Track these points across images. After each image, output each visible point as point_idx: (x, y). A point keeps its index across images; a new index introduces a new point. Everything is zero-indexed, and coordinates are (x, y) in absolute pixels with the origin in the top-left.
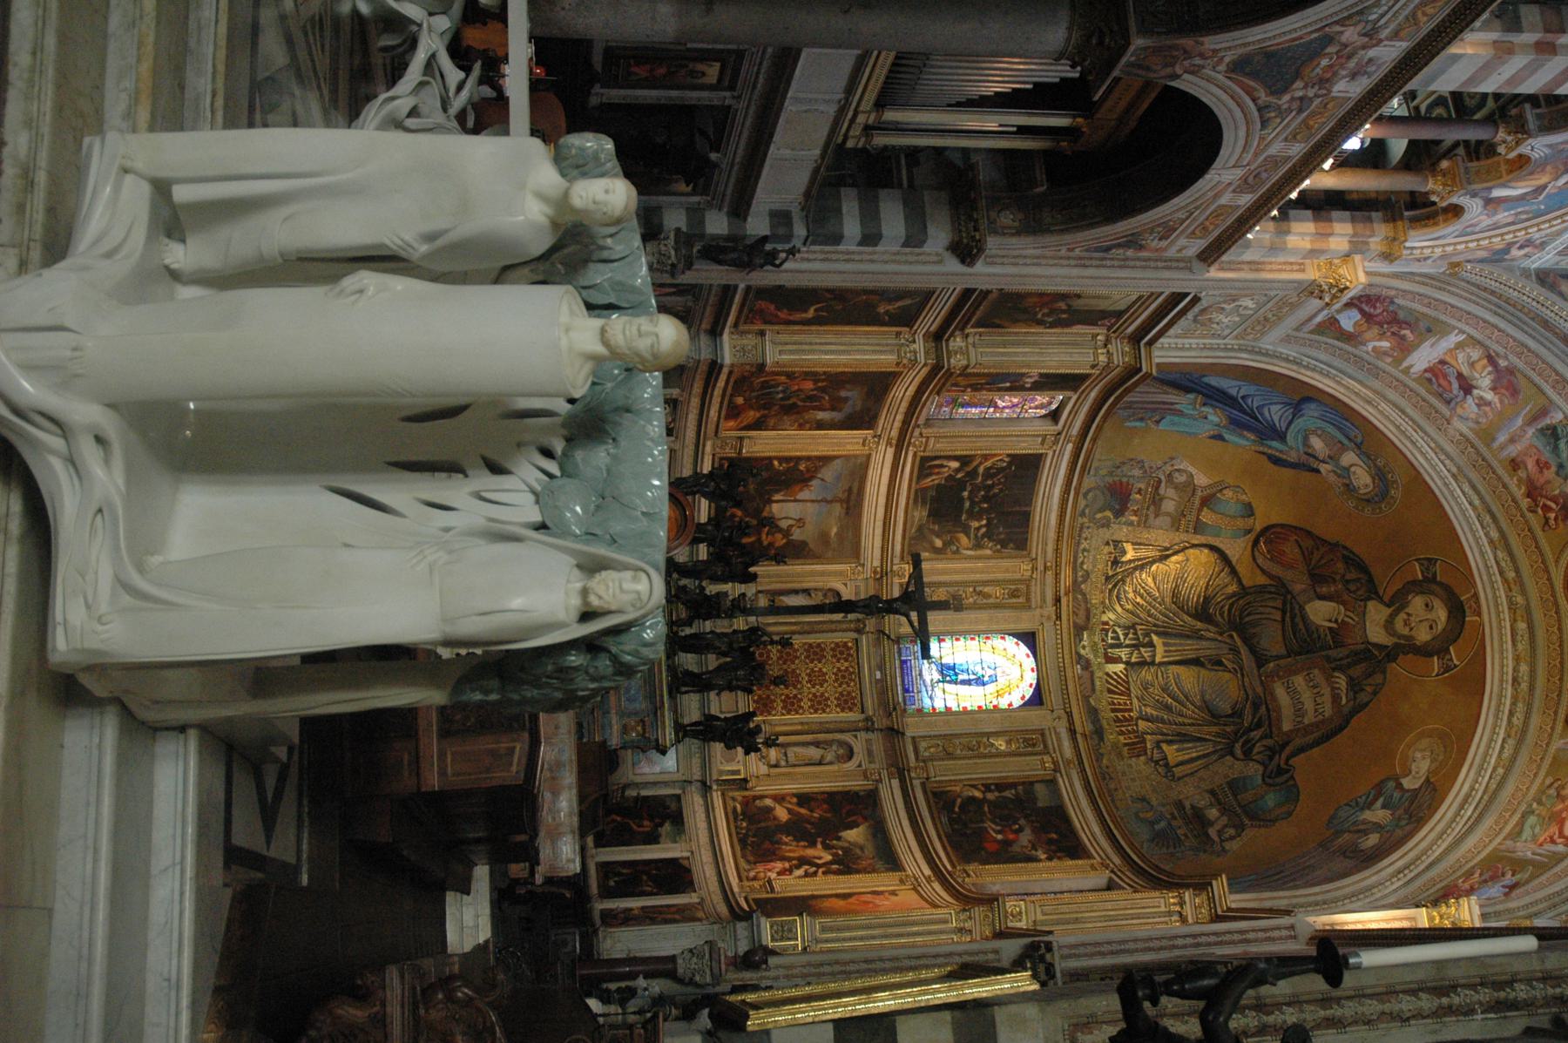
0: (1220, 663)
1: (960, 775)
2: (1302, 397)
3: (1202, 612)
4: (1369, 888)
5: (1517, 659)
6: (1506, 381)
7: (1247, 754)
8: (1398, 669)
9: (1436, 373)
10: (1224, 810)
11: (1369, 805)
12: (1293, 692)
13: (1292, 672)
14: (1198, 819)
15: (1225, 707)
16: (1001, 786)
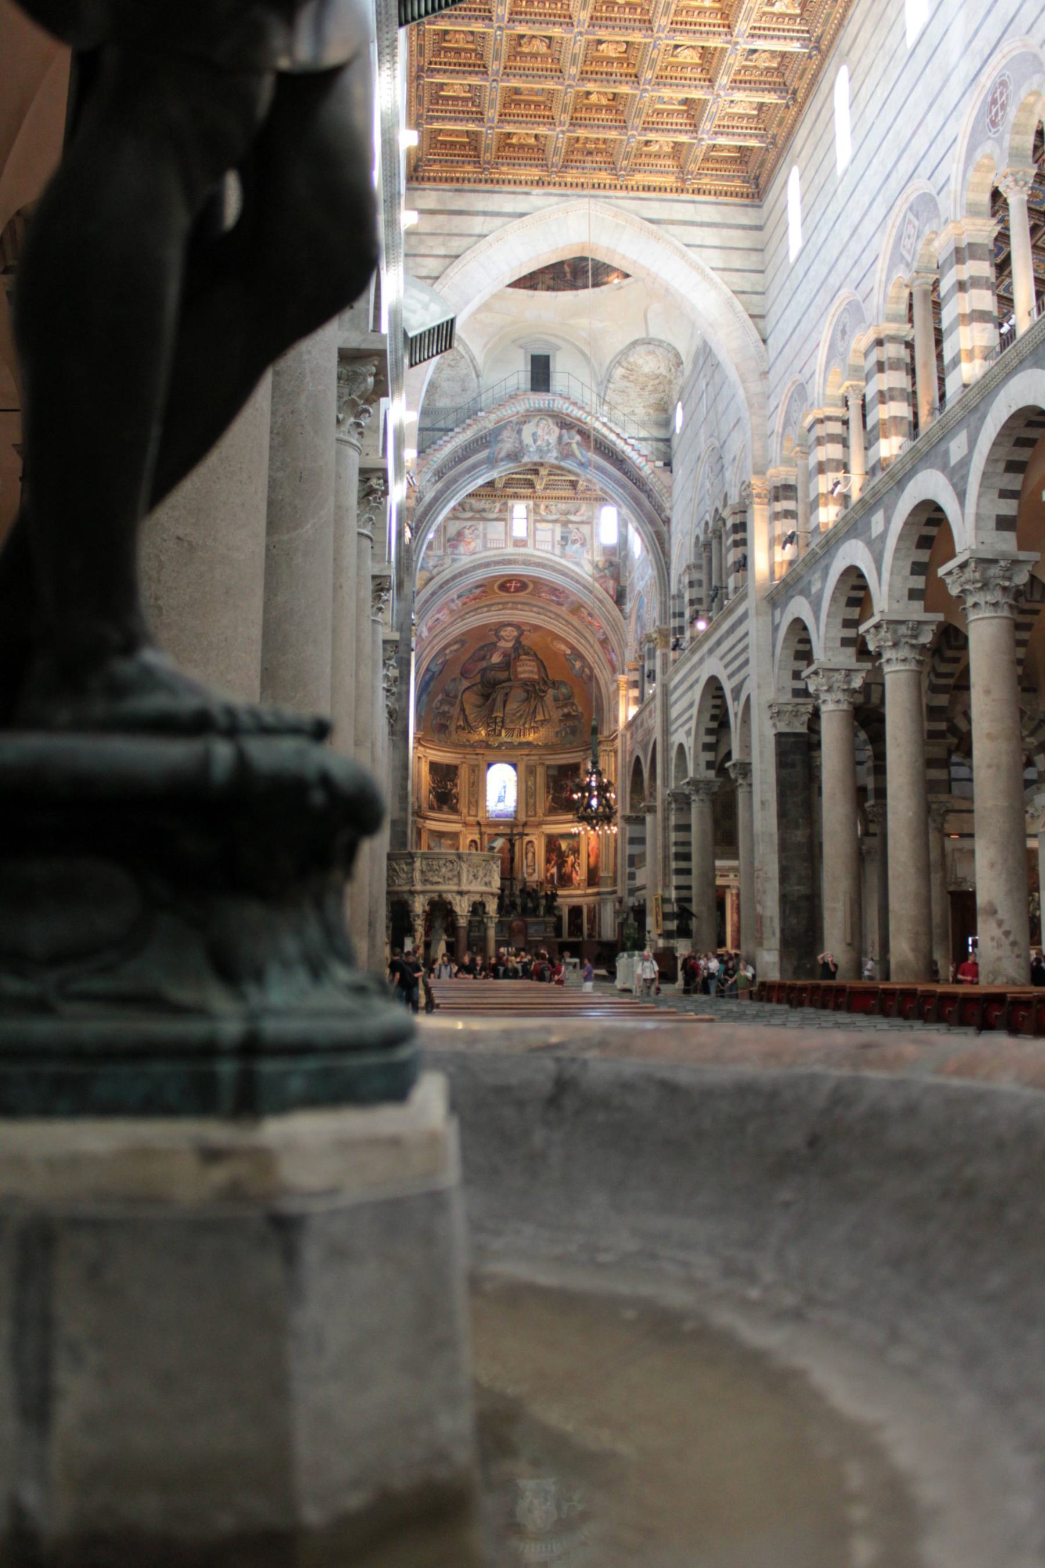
0: (507, 694)
1: (543, 801)
2: (428, 670)
3: (486, 697)
4: (606, 683)
5: (532, 611)
6: (439, 612)
7: (544, 692)
8: (525, 642)
9: (430, 629)
10: (565, 706)
11: (574, 665)
12: (524, 672)
13: (516, 671)
14: (567, 716)
15: (524, 695)
16: (548, 787)
